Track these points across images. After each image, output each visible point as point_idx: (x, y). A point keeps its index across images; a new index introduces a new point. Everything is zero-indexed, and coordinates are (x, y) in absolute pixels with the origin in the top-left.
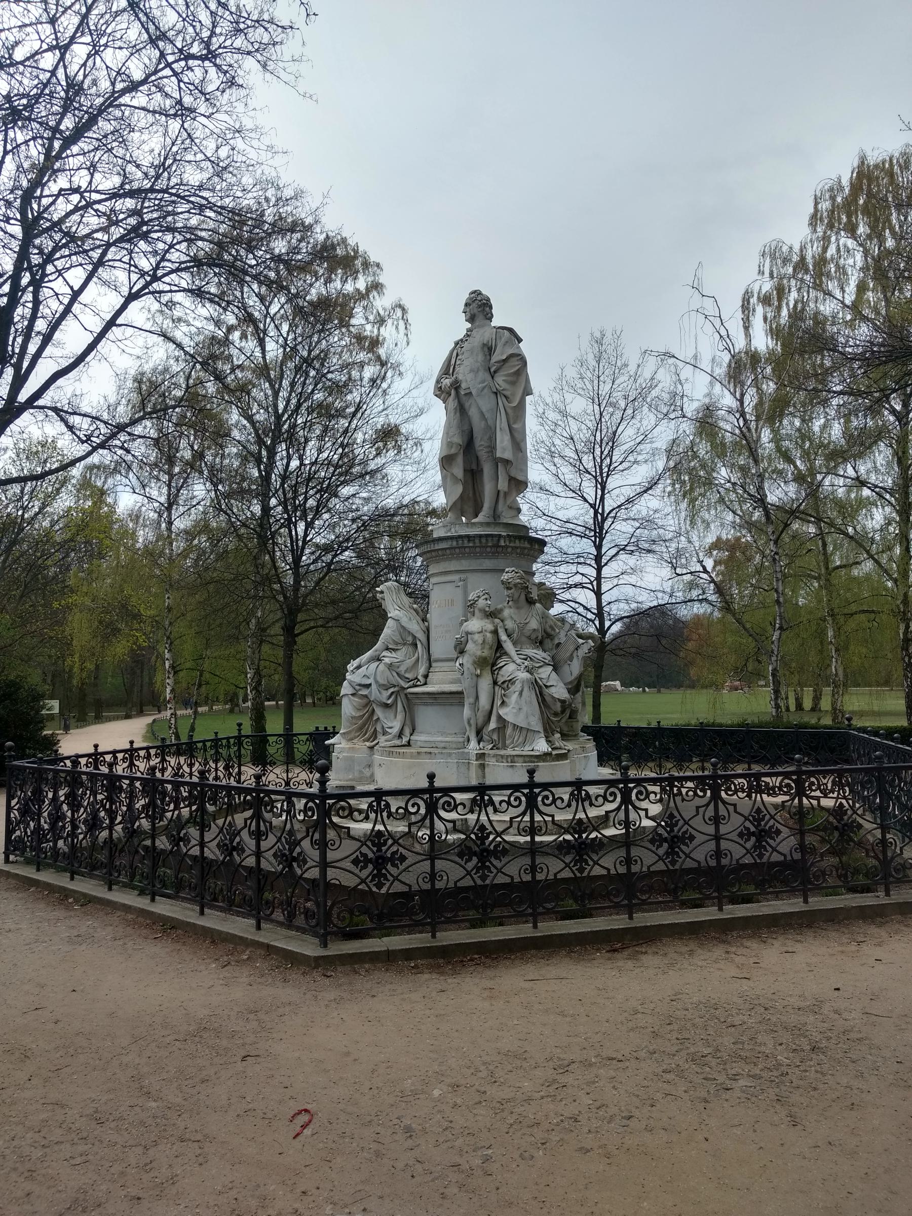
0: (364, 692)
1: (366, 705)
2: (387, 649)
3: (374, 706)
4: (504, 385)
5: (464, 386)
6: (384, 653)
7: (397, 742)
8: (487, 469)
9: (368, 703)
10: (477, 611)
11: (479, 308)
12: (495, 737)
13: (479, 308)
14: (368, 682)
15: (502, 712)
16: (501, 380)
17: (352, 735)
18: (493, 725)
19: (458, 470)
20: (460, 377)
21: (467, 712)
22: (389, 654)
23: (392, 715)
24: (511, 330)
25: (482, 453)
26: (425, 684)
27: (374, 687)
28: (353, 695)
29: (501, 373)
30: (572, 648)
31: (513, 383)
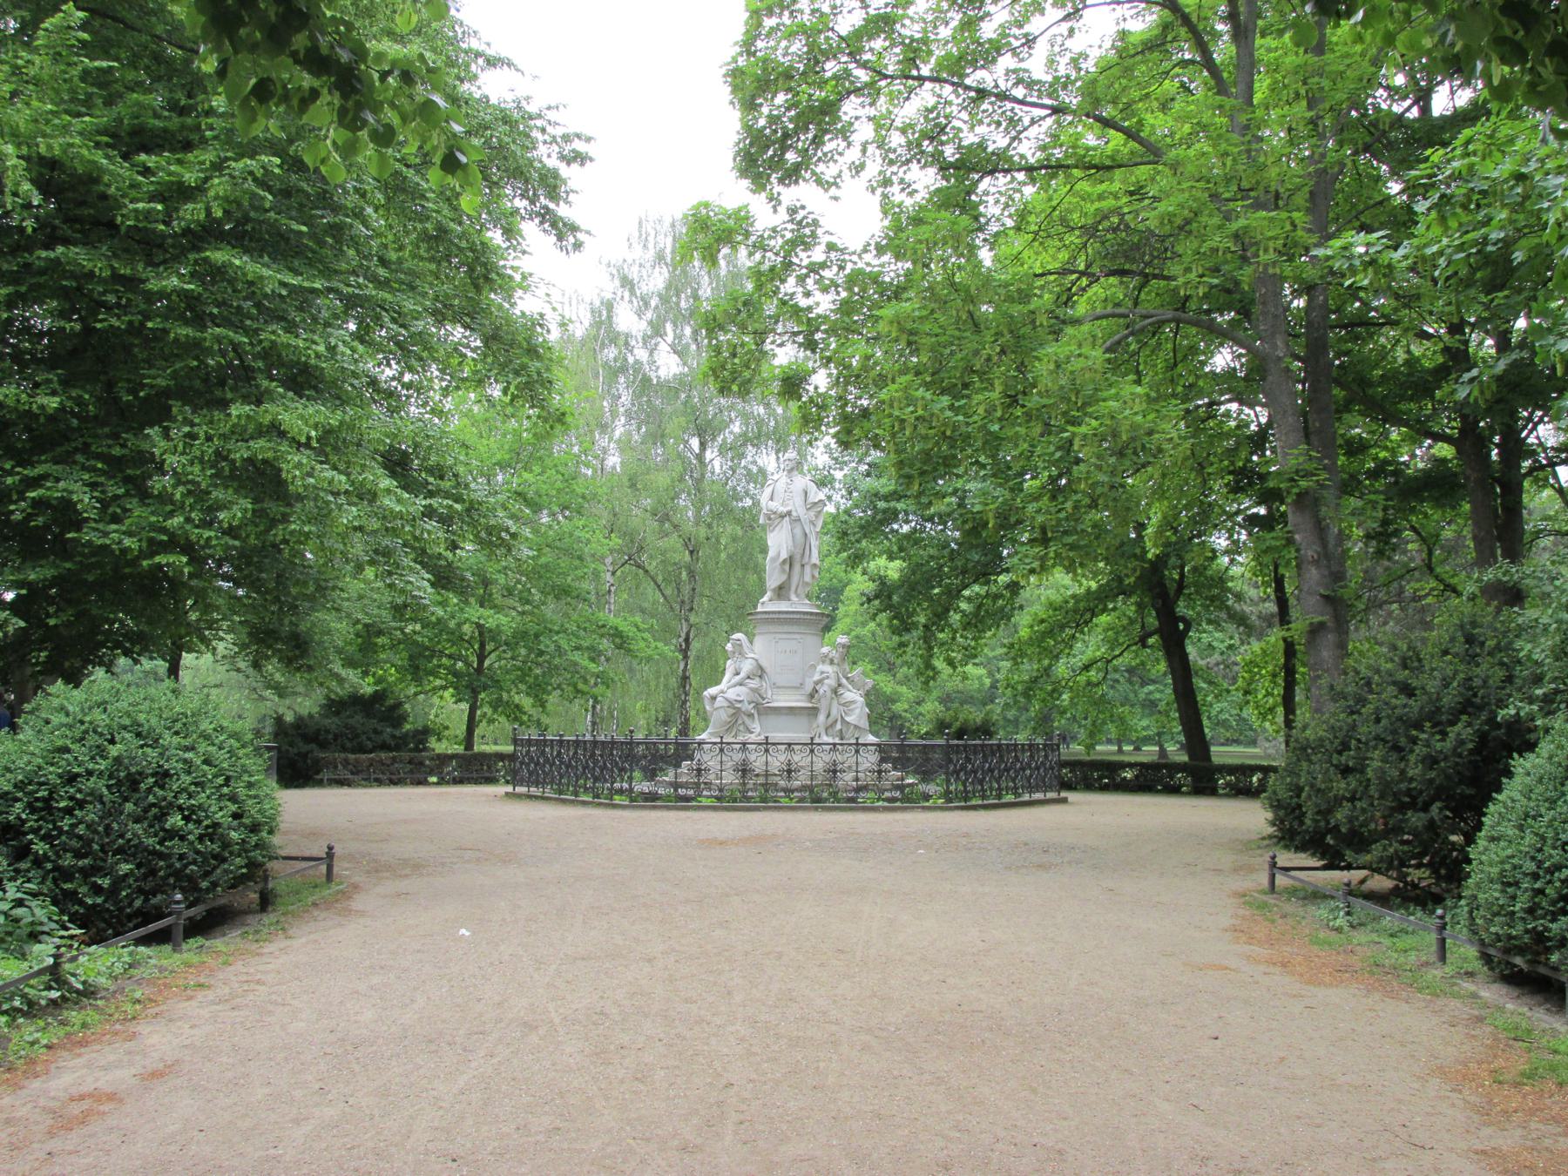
8: (797, 568)
16: (812, 514)
18: (839, 726)
21: (821, 717)
25: (798, 557)
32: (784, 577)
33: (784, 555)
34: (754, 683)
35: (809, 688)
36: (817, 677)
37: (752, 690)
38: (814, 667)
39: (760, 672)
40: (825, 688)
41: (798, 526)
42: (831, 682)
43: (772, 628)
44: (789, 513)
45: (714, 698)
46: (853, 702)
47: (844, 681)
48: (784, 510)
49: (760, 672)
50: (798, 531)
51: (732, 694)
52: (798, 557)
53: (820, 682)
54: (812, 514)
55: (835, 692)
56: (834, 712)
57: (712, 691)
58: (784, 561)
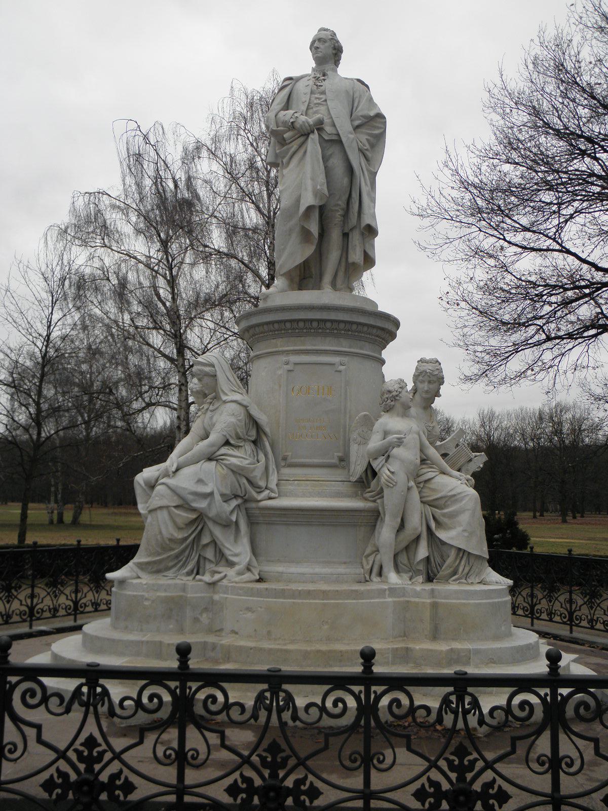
0: (202, 504)
1: (193, 522)
2: (227, 443)
3: (210, 524)
4: (368, 146)
5: (328, 129)
6: (224, 450)
7: (247, 576)
8: (335, 235)
9: (200, 520)
10: (398, 405)
11: (328, 51)
12: (421, 567)
13: (328, 51)
14: (208, 490)
15: (442, 535)
17: (162, 566)
18: (423, 552)
19: (314, 229)
20: (327, 120)
21: (386, 534)
22: (231, 452)
23: (232, 538)
24: (367, 86)
26: (280, 496)
27: (217, 497)
28: (176, 507)
29: (363, 130)
30: (463, 460)
31: (373, 146)
32: (309, 250)
33: (308, 200)
34: (240, 457)
35: (357, 468)
36: (375, 442)
37: (236, 471)
38: (368, 423)
39: (254, 433)
40: (394, 466)
41: (334, 150)
42: (407, 454)
43: (280, 344)
44: (319, 126)
45: (151, 486)
46: (452, 498)
47: (433, 452)
48: (311, 121)
49: (254, 433)
50: (337, 163)
51: (185, 480)
52: (338, 216)
53: (385, 453)
54: (364, 138)
55: (416, 476)
56: (415, 522)
57: (149, 473)
58: (310, 209)
